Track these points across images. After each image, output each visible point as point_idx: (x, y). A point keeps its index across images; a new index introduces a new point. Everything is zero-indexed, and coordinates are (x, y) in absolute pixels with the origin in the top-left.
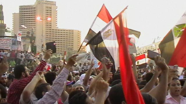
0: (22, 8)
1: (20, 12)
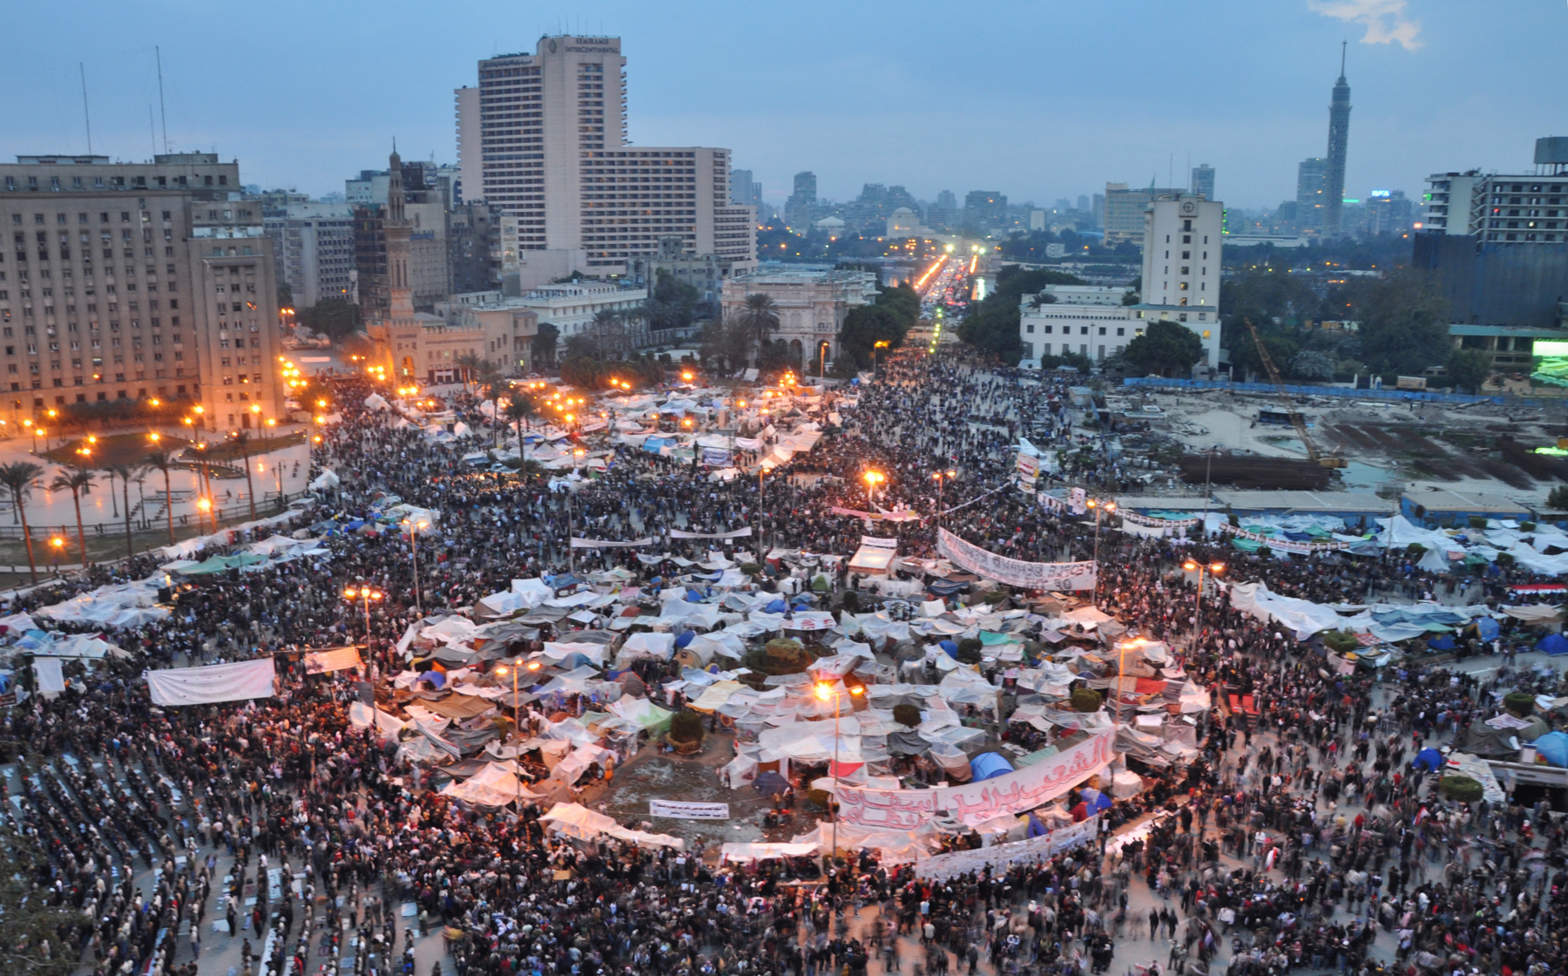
0: (489, 70)
1: (482, 84)
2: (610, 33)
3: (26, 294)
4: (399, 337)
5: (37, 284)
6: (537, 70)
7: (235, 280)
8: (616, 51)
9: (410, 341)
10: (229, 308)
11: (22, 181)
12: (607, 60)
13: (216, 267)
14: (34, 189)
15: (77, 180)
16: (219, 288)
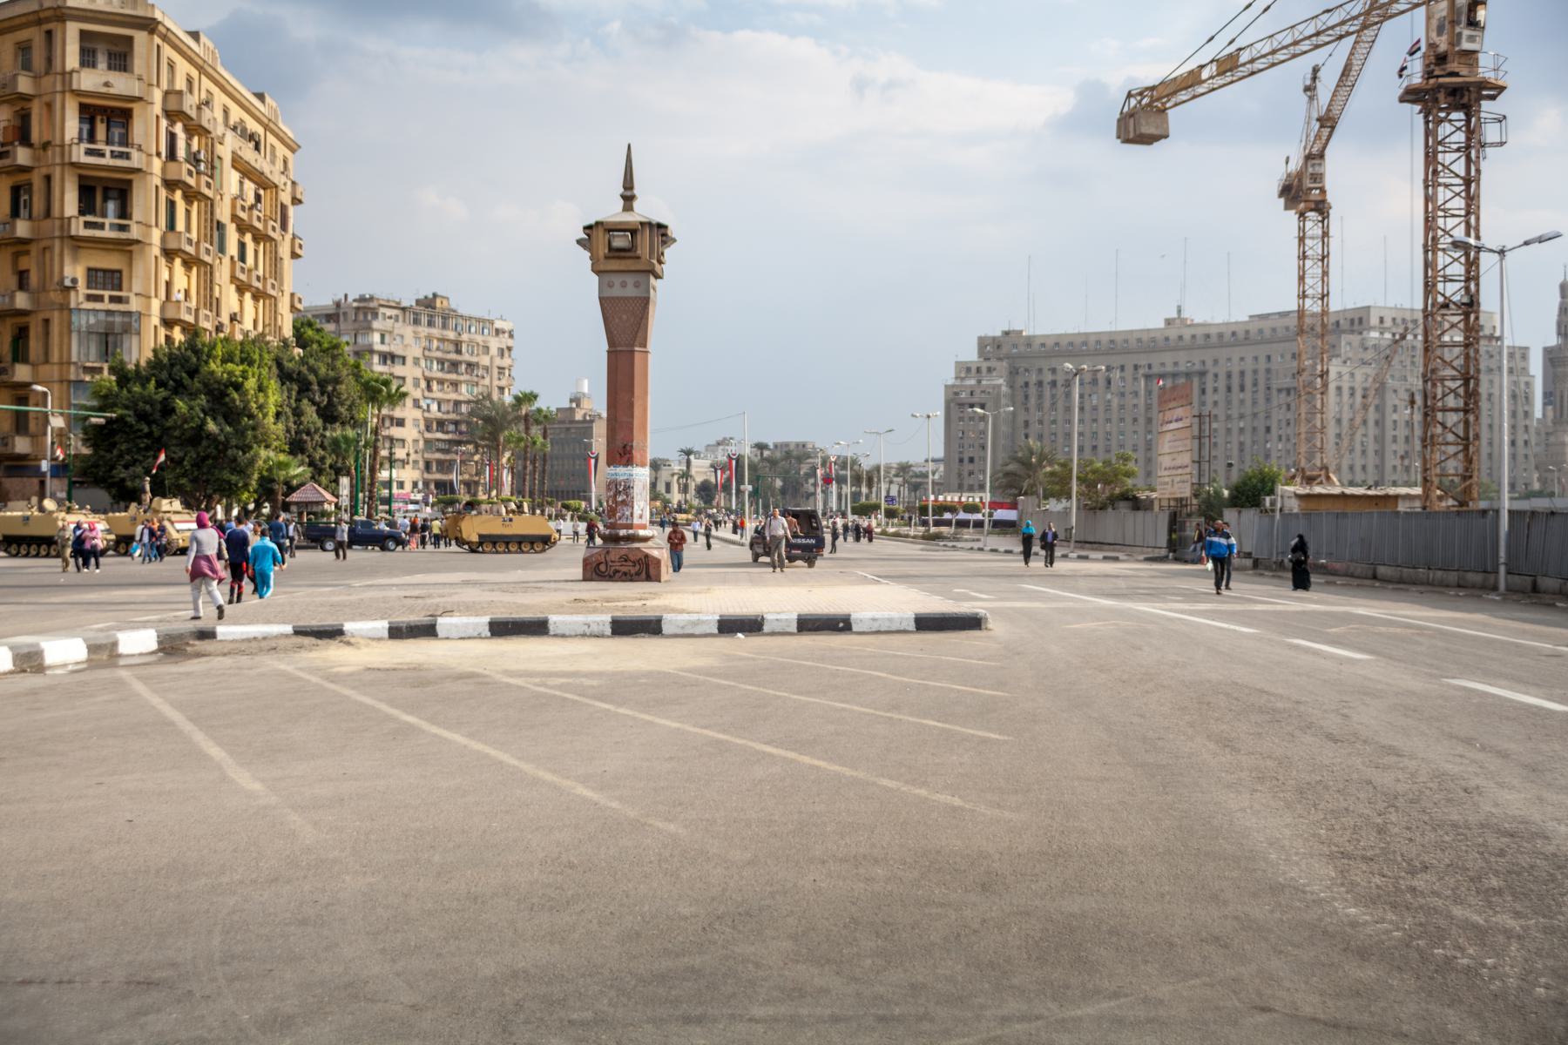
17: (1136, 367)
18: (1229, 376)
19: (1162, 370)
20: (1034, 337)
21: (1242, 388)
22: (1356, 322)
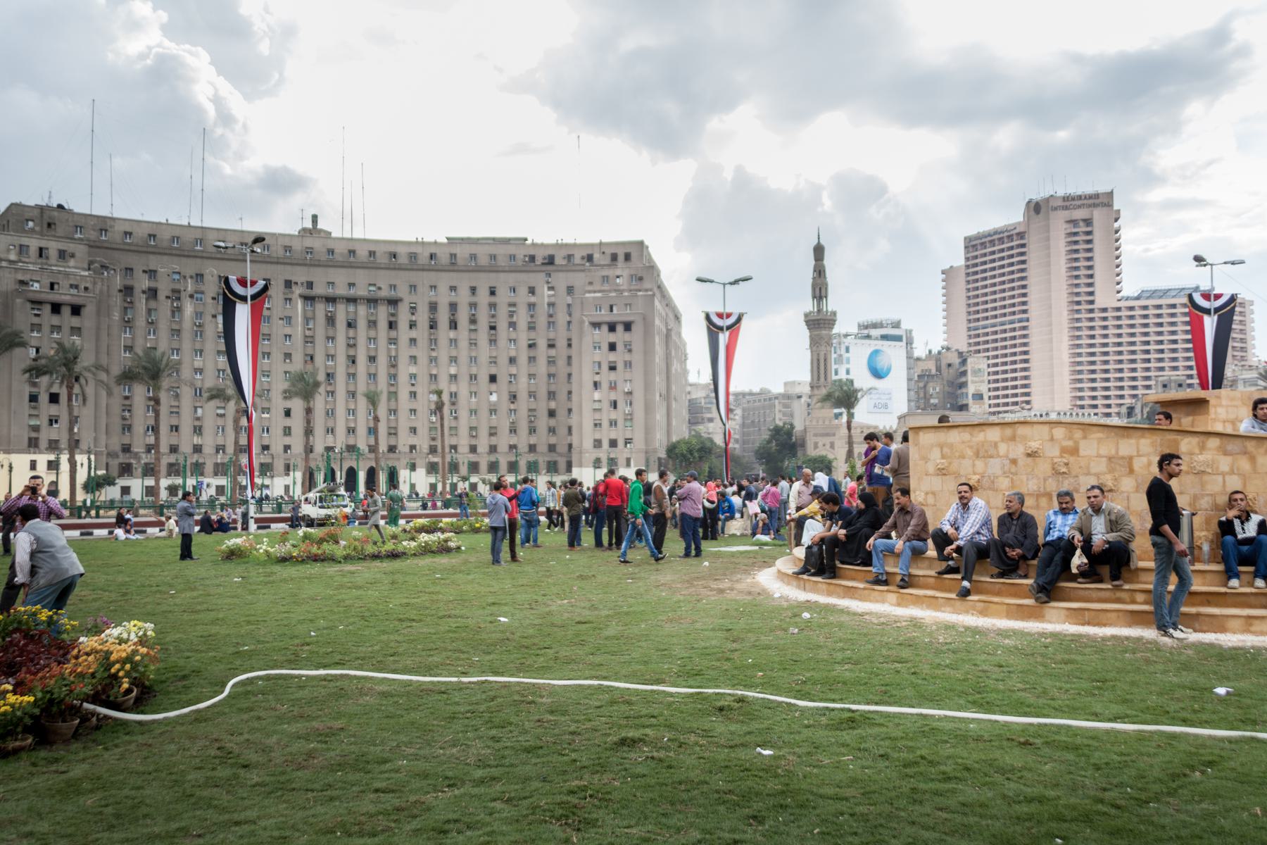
1: (967, 259)
2: (1102, 189)
3: (433, 360)
4: (816, 435)
5: (443, 353)
6: (1021, 235)
7: (612, 338)
8: (1109, 205)
9: (827, 440)
10: (605, 367)
11: (444, 258)
12: (1097, 215)
13: (596, 325)
14: (453, 264)
15: (493, 257)
16: (597, 346)
17: (288, 284)
18: (433, 307)
19: (330, 291)
20: (113, 219)
21: (454, 325)
22: (621, 258)
